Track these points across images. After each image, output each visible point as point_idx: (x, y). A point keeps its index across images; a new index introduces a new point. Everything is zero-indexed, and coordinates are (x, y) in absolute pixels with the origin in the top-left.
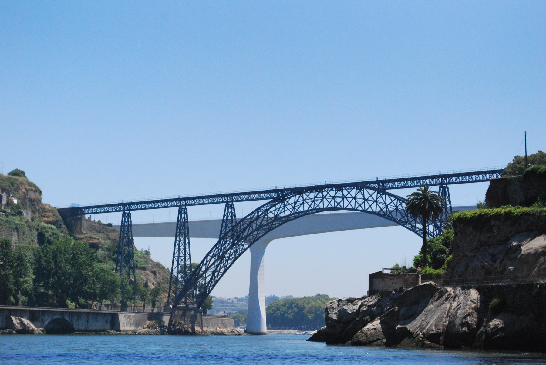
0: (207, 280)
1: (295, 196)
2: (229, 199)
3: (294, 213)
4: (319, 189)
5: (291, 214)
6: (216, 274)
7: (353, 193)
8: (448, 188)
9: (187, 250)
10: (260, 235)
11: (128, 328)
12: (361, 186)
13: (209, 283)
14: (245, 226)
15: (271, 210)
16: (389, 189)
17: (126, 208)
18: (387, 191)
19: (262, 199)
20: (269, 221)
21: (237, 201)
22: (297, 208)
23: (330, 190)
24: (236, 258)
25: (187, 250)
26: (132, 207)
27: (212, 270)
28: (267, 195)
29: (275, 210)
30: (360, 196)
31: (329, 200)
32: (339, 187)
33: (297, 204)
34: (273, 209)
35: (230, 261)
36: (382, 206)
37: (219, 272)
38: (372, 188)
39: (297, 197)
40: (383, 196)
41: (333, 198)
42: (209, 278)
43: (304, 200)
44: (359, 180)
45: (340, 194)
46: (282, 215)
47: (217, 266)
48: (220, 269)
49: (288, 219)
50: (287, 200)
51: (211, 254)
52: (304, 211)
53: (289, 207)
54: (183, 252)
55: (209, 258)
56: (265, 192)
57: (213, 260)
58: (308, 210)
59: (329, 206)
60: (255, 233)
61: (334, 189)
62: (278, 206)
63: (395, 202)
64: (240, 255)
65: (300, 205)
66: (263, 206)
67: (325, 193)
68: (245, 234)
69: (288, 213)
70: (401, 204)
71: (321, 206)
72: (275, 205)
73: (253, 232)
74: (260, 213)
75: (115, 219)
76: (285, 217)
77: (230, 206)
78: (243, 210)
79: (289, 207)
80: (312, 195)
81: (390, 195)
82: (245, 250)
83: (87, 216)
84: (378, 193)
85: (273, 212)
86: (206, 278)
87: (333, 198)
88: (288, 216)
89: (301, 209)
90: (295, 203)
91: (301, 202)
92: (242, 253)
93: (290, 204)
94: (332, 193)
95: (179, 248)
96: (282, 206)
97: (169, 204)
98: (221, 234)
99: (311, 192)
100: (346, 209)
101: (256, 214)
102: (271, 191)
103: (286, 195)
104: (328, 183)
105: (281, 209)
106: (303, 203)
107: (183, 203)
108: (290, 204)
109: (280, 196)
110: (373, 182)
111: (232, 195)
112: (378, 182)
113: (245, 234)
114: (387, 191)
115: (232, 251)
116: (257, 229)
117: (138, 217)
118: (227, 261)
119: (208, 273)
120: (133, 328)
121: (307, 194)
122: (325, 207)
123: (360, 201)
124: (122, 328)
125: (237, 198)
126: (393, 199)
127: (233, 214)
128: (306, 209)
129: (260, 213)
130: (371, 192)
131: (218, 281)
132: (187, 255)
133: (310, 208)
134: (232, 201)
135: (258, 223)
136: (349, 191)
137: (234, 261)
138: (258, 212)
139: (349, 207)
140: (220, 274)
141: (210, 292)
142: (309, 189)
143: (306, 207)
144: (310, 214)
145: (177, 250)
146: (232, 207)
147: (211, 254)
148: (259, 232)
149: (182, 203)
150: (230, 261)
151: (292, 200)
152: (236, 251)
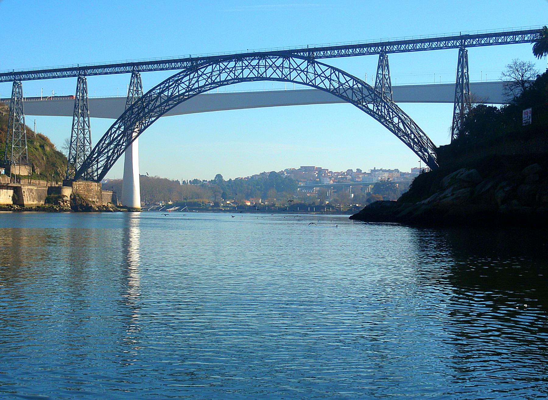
1: (212, 64)
2: (135, 68)
4: (239, 57)
5: (205, 85)
10: (171, 106)
11: (31, 202)
12: (287, 54)
13: (111, 156)
16: (320, 57)
18: (316, 60)
19: (173, 69)
20: (180, 93)
21: (24, 79)
22: (213, 78)
23: (252, 60)
29: (189, 80)
30: (286, 64)
33: (214, 74)
37: (122, 145)
39: (214, 65)
41: (254, 68)
42: (111, 151)
45: (262, 62)
46: (196, 86)
49: (201, 89)
50: (202, 70)
51: (117, 126)
52: (220, 81)
54: (82, 125)
55: (114, 130)
58: (225, 81)
59: (251, 75)
60: (165, 105)
62: (192, 75)
66: (174, 76)
69: (202, 83)
70: (334, 72)
73: (162, 104)
76: (199, 87)
77: (135, 75)
78: (150, 81)
79: (205, 77)
80: (232, 64)
81: (317, 63)
85: (187, 83)
86: (108, 152)
89: (218, 80)
90: (212, 72)
91: (218, 72)
92: (148, 126)
93: (205, 74)
94: (254, 63)
96: (196, 75)
99: (229, 62)
100: (270, 79)
101: (167, 85)
103: (202, 64)
106: (219, 75)
107: (136, 68)
108: (205, 74)
109: (194, 65)
110: (303, 51)
112: (309, 50)
114: (316, 60)
116: (167, 101)
119: (112, 146)
120: (36, 202)
121: (226, 64)
122: (268, 77)
124: (25, 203)
127: (20, 93)
129: (170, 83)
130: (299, 61)
133: (229, 78)
134: (139, 71)
136: (274, 60)
138: (169, 82)
139: (275, 76)
140: (123, 147)
141: (111, 166)
142: (228, 58)
143: (223, 77)
144: (228, 84)
147: (117, 126)
148: (170, 102)
149: (81, 72)
151: (209, 69)
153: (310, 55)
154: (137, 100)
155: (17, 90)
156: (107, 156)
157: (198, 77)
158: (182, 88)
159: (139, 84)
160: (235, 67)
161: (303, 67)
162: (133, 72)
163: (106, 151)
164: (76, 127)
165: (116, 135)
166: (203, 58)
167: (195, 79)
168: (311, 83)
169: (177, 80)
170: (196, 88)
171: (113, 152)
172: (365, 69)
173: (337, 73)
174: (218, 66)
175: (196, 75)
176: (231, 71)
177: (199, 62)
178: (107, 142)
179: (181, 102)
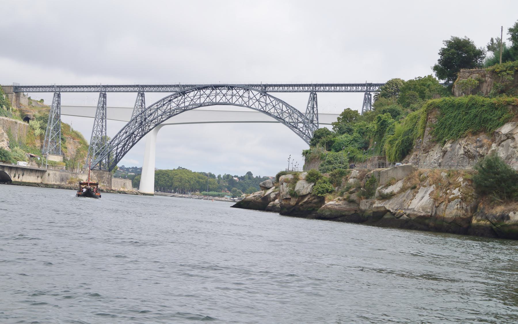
0: (118, 151)
2: (141, 90)
3: (192, 105)
6: (126, 146)
7: (241, 92)
8: (316, 95)
9: (104, 126)
10: (164, 119)
12: (247, 88)
13: (119, 153)
14: (152, 111)
15: (174, 100)
17: (57, 90)
24: (143, 136)
25: (104, 126)
26: (62, 89)
27: (123, 144)
28: (172, 89)
31: (222, 97)
32: (231, 87)
33: (196, 97)
34: (176, 99)
35: (137, 138)
36: (263, 105)
38: (257, 90)
39: (196, 92)
40: (265, 97)
41: (224, 95)
42: (120, 149)
43: (201, 95)
44: (247, 83)
45: (230, 92)
46: (183, 105)
47: (127, 141)
48: (129, 143)
53: (189, 99)
55: (122, 133)
56: (170, 86)
57: (125, 135)
59: (221, 101)
61: (226, 88)
62: (180, 98)
63: (274, 102)
64: (145, 134)
65: (198, 99)
67: (218, 91)
68: (152, 117)
69: (187, 104)
71: (214, 101)
72: (177, 97)
74: (165, 102)
75: (48, 98)
78: (152, 98)
79: (189, 99)
80: (208, 92)
81: (269, 96)
82: (151, 130)
83: (25, 93)
84: (261, 94)
86: (117, 149)
87: (224, 95)
88: (187, 107)
89: (198, 102)
91: (199, 97)
92: (148, 132)
94: (224, 92)
95: (98, 125)
97: (93, 89)
98: (133, 116)
100: (234, 104)
101: (162, 103)
102: (174, 86)
104: (222, 83)
105: (182, 100)
106: (200, 98)
109: (183, 90)
111: (143, 86)
113: (152, 117)
115: (140, 130)
117: (66, 98)
118: (135, 137)
121: (204, 90)
123: (246, 99)
125: (147, 89)
126: (272, 99)
128: (202, 102)
129: (165, 102)
130: (255, 93)
131: (126, 152)
132: (104, 130)
135: (163, 111)
136: (238, 91)
137: (141, 138)
139: (237, 103)
141: (119, 160)
142: (206, 87)
145: (96, 125)
146: (143, 95)
147: (124, 131)
150: (137, 138)
151: (192, 94)
152: (143, 130)
153: (264, 89)
154: (140, 112)
155: (102, 99)
156: (116, 153)
157: (185, 99)
158: (173, 105)
159: (143, 101)
160: (209, 94)
161: (258, 97)
162: (139, 92)
163: (115, 148)
164: (95, 129)
165: (123, 137)
166: (192, 86)
167: (182, 100)
168: (262, 110)
169: (170, 101)
170: (182, 107)
171: (122, 150)
172: (300, 101)
173: (281, 104)
174: (199, 93)
175: (183, 98)
176: (208, 97)
177: (186, 88)
178: (116, 142)
179: (172, 116)
